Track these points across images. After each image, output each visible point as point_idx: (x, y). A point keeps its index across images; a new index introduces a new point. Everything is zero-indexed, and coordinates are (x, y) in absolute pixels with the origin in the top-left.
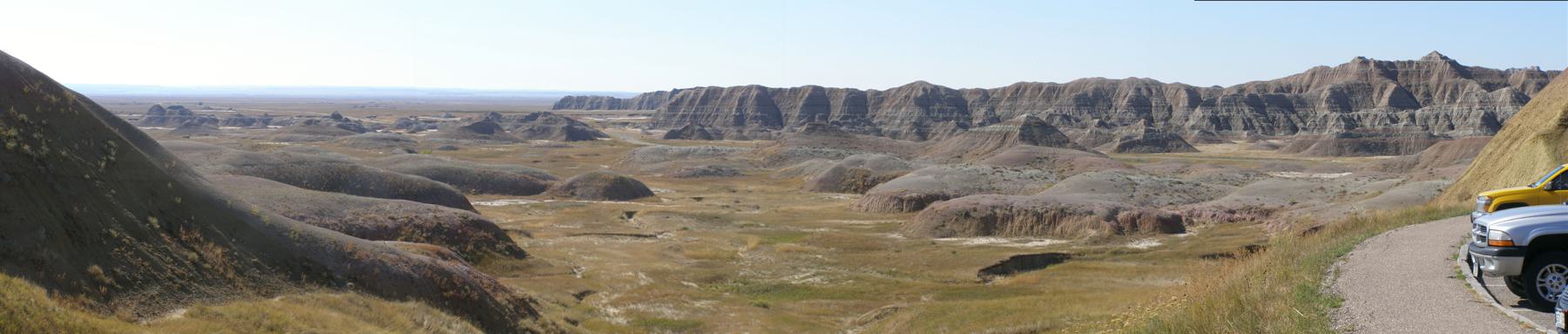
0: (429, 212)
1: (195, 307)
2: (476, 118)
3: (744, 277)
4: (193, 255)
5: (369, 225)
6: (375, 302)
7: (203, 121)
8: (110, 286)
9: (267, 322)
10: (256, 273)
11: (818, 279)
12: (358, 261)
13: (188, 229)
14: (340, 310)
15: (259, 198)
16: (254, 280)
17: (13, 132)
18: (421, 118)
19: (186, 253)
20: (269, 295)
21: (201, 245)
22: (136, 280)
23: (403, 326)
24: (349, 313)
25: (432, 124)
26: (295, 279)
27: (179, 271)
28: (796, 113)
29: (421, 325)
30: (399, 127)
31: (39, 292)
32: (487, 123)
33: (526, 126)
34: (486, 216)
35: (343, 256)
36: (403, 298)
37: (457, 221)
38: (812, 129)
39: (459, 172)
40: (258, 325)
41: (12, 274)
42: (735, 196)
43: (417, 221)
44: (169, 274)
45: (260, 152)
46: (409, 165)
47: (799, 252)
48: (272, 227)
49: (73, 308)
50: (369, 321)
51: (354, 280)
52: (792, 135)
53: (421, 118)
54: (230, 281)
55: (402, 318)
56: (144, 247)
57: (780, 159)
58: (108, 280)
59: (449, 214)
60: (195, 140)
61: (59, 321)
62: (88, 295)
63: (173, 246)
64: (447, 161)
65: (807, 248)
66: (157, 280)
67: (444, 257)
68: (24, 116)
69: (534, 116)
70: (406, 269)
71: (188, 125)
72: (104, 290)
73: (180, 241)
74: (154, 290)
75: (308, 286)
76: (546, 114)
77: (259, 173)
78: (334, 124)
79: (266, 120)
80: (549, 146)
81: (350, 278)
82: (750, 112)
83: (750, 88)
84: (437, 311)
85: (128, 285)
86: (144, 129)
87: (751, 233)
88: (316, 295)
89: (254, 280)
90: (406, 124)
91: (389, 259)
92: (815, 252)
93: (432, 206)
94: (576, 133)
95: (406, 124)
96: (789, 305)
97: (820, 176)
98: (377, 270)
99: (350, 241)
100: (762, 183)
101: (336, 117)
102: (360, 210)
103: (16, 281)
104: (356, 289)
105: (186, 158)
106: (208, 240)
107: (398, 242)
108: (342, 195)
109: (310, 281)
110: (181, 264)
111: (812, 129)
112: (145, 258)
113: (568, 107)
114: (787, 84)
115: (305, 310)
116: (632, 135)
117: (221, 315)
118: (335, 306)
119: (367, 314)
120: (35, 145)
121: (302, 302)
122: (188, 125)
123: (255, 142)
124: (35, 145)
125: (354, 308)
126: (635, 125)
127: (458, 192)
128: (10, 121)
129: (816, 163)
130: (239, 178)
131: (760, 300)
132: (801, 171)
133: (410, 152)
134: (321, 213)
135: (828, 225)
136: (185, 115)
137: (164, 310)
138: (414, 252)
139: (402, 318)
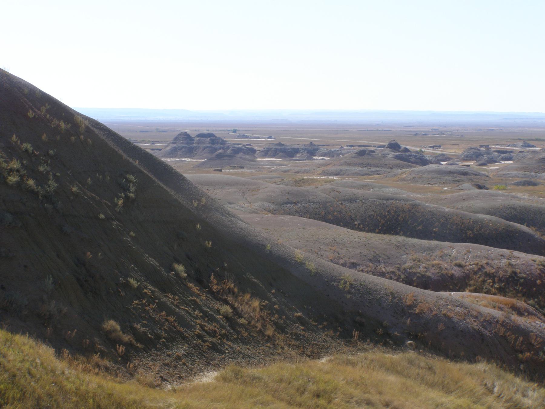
0: (501, 259)
1: (228, 370)
4: (226, 309)
5: (432, 273)
6: (439, 363)
7: (237, 151)
8: (129, 345)
9: (312, 387)
10: (299, 329)
12: (419, 316)
13: (220, 278)
14: (398, 373)
15: (304, 242)
16: (298, 337)
17: (15, 164)
18: (493, 147)
19: (217, 306)
20: (315, 355)
21: (235, 295)
22: (159, 337)
23: (472, 393)
24: (408, 376)
25: (506, 155)
26: (346, 337)
27: (209, 327)
29: (491, 391)
30: (467, 158)
31: (46, 352)
35: (402, 309)
36: (472, 359)
37: (536, 269)
40: (302, 391)
41: (14, 330)
43: (488, 269)
44: (198, 330)
45: (305, 188)
46: (479, 204)
48: (318, 275)
49: (86, 371)
50: (432, 385)
51: (415, 338)
53: (493, 147)
54: (269, 339)
55: (470, 382)
56: (168, 299)
58: (126, 338)
60: (228, 174)
61: (69, 386)
62: (103, 355)
63: (202, 298)
64: (524, 198)
66: (184, 338)
67: (520, 313)
68: (27, 146)
70: (476, 325)
71: (220, 157)
72: (121, 349)
73: (211, 292)
74: (181, 350)
75: (360, 345)
77: (303, 213)
78: (391, 154)
79: (311, 151)
81: (409, 336)
84: (510, 376)
85: (148, 344)
86: (169, 160)
88: (370, 356)
89: (298, 337)
90: (475, 155)
91: (455, 313)
93: (506, 252)
95: (475, 155)
98: (441, 326)
99: (409, 292)
101: (394, 146)
102: (421, 256)
103: (19, 338)
104: (416, 348)
105: (218, 195)
106: (243, 291)
107: (466, 293)
108: (401, 239)
109: (363, 338)
110: (212, 319)
112: (171, 312)
115: (357, 373)
117: (259, 379)
118: (392, 369)
119: (429, 377)
120: (41, 179)
121: (353, 364)
122: (220, 157)
123: (299, 176)
124: (41, 179)
125: (414, 371)
128: (12, 152)
130: (280, 218)
133: (480, 187)
134: (375, 260)
136: (215, 145)
137: (192, 373)
138: (483, 305)
139: (470, 382)
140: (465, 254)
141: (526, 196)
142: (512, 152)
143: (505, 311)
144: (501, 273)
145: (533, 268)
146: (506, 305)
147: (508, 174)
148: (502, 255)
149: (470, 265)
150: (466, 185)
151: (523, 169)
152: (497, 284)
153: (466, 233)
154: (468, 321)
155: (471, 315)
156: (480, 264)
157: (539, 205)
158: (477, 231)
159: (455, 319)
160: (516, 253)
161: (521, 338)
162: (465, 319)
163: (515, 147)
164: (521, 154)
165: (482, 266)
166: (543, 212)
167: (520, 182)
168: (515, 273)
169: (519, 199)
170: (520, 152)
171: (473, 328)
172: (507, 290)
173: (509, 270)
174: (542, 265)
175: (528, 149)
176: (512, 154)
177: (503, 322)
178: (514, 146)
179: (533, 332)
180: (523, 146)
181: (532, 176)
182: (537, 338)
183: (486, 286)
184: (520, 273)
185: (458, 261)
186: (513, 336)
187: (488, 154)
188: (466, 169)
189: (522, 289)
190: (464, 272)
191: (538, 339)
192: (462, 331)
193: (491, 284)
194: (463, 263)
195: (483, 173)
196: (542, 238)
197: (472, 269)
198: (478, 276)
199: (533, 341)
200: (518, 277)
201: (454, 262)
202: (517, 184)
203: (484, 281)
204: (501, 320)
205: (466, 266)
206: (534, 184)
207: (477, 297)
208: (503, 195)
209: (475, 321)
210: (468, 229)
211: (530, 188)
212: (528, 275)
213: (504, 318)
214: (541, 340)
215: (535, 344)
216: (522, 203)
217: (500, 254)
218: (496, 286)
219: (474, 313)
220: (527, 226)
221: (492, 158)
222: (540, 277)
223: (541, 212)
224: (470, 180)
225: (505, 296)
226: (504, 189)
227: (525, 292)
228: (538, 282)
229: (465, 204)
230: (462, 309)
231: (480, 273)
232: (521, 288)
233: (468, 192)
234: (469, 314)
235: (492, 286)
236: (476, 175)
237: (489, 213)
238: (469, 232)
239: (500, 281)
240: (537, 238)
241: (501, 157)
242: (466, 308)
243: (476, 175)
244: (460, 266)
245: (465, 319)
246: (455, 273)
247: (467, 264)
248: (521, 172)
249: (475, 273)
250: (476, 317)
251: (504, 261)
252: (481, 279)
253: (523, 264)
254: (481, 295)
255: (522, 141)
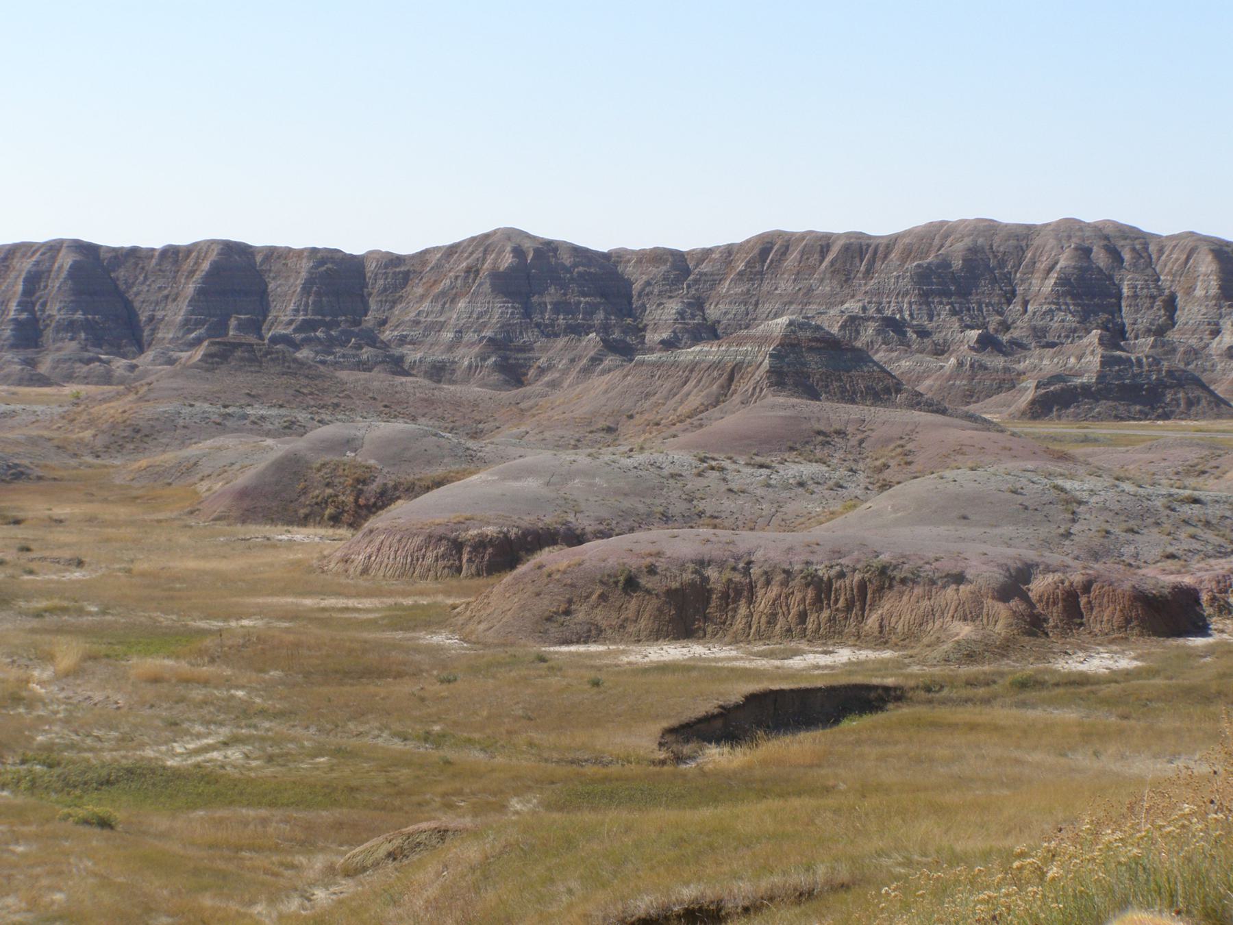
3: (49, 747)
11: (235, 754)
28: (178, 312)
38: (220, 357)
42: (19, 533)
47: (186, 681)
52: (166, 373)
57: (135, 436)
65: (207, 670)
82: (55, 311)
83: (54, 248)
87: (60, 630)
92: (229, 683)
96: (161, 822)
97: (242, 480)
100: (90, 497)
111: (220, 357)
114: (153, 238)
129: (231, 444)
131: (91, 808)
132: (188, 469)
135: (261, 612)
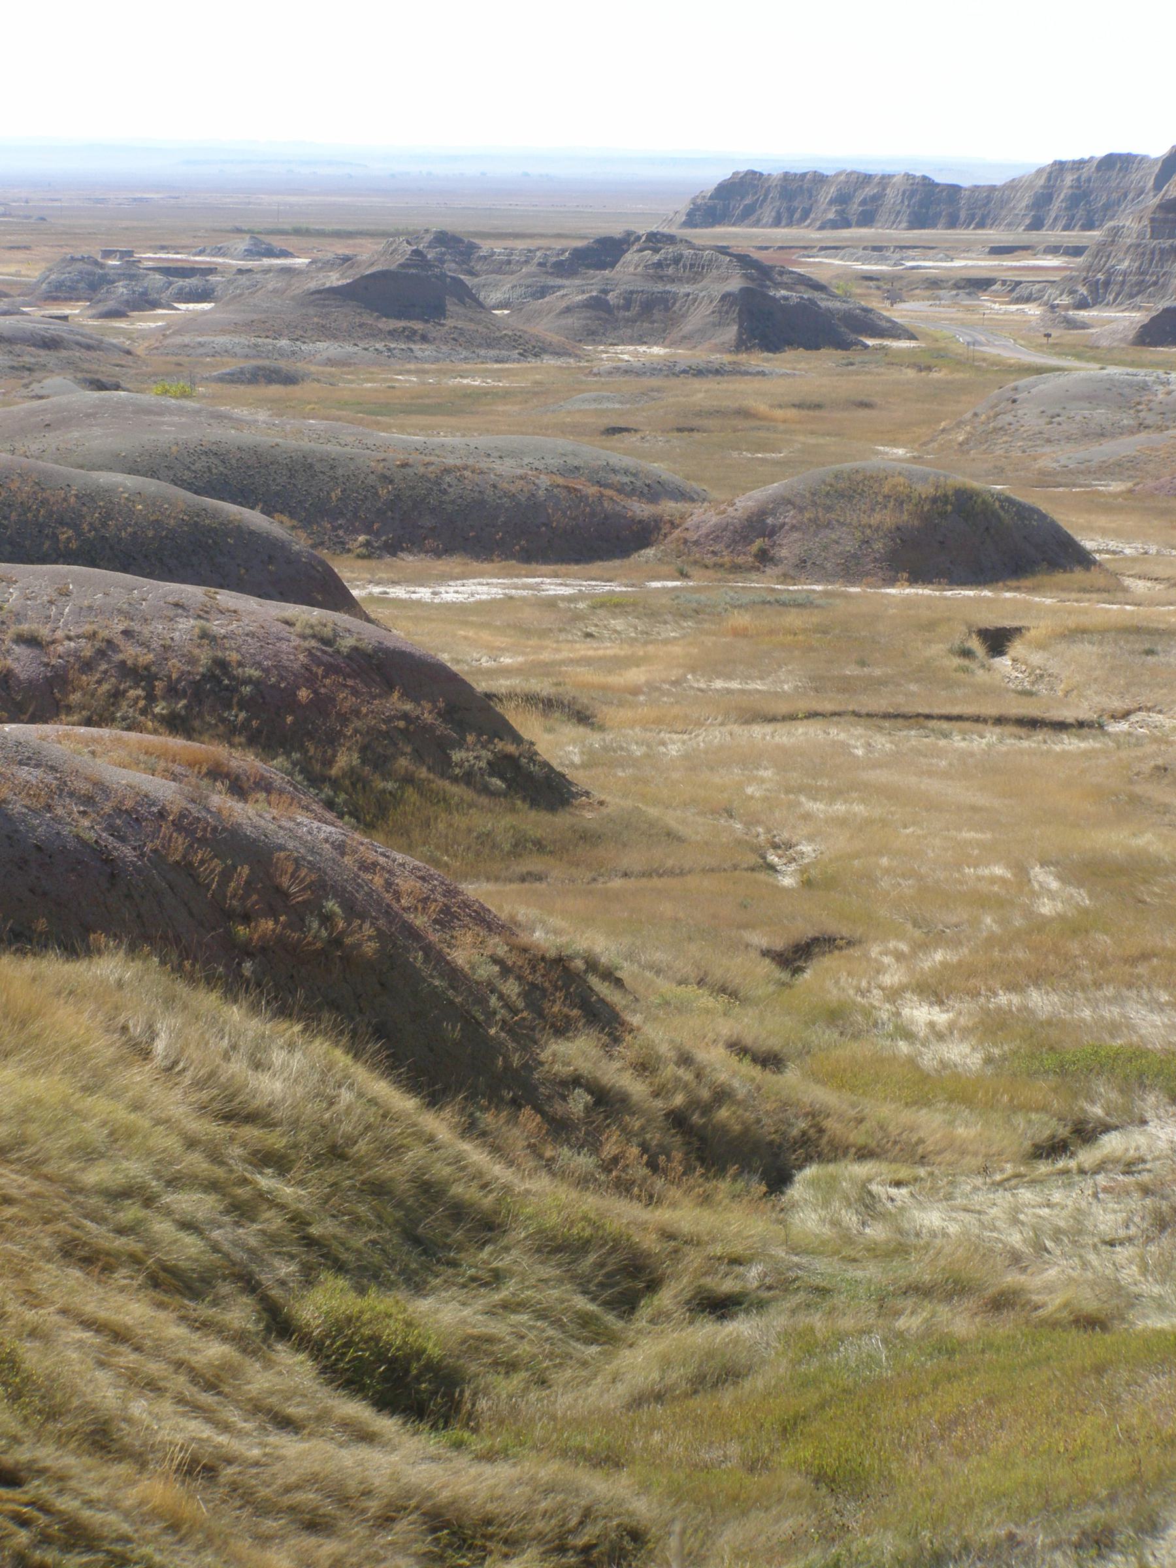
0: (177, 617)
2: (371, 256)
18: (148, 257)
25: (193, 283)
30: (59, 292)
32: (418, 283)
33: (574, 290)
34: (405, 635)
37: (293, 651)
39: (303, 467)
43: (130, 652)
46: (98, 438)
53: (148, 257)
59: (254, 622)
64: (256, 423)
67: (239, 788)
69: (605, 251)
70: (87, 827)
76: (655, 240)
80: (670, 370)
90: (87, 282)
93: (193, 593)
94: (777, 318)
95: (87, 282)
113: (747, 215)
116: (1003, 329)
126: (1016, 291)
127: (300, 542)
133: (100, 386)
140: (51, 602)
141: (262, 416)
142: (211, 271)
143: (189, 784)
144: (175, 665)
145: (284, 646)
146: (191, 765)
147: (201, 345)
148: (177, 605)
149: (69, 638)
150: (54, 381)
151: (248, 326)
152: (164, 704)
153: (55, 536)
154: (60, 811)
155: (71, 794)
156: (104, 634)
157: (306, 445)
158: (92, 527)
159: (17, 807)
160: (227, 598)
161: (246, 871)
162: (49, 808)
163: (224, 255)
164: (243, 280)
165: (109, 642)
166: (318, 467)
167: (242, 372)
168: (222, 664)
169: (238, 423)
170: (240, 271)
171: (77, 837)
172: (197, 724)
173: (204, 657)
174: (314, 636)
175: (267, 262)
176: (212, 278)
177: (182, 816)
178: (220, 252)
179: (282, 848)
180: (250, 253)
181: (281, 353)
182: (298, 867)
183: (124, 709)
184: (240, 664)
185: (25, 627)
186: (217, 865)
187: (132, 277)
188: (57, 329)
189: (248, 720)
190: (47, 665)
191: (303, 872)
192: (39, 848)
193: (142, 703)
194: (44, 632)
195: (115, 341)
196: (315, 552)
197: (76, 653)
198: (98, 676)
199: (285, 881)
200: (232, 678)
201: (13, 630)
202: (233, 378)
203: (116, 695)
204: (175, 809)
205: (53, 642)
206: (289, 379)
207: (94, 740)
208: (181, 411)
209: (84, 813)
210: (62, 523)
211: (276, 390)
212: (266, 671)
213: (185, 804)
214: (314, 877)
215: (293, 889)
216: (247, 437)
217: (170, 599)
218: (157, 710)
219: (83, 787)
220: (263, 512)
221: (145, 294)
222: (310, 680)
223: (311, 466)
224: (70, 364)
225: (190, 738)
226: (184, 395)
227: (259, 731)
228: (303, 694)
229: (52, 440)
230: (39, 772)
231: (104, 667)
232: (243, 715)
233: (63, 399)
234: (62, 790)
235: (144, 712)
236: (89, 347)
237: (132, 471)
238: (65, 534)
239: (173, 692)
240: (299, 554)
241: (173, 289)
242: (53, 769)
243: (89, 347)
244: (31, 641)
245: (49, 808)
246: (16, 667)
247: (59, 634)
248: (243, 340)
249: (87, 666)
250: (89, 800)
251: (186, 626)
252: (106, 687)
253: (251, 635)
254: (105, 732)
255: (247, 237)
